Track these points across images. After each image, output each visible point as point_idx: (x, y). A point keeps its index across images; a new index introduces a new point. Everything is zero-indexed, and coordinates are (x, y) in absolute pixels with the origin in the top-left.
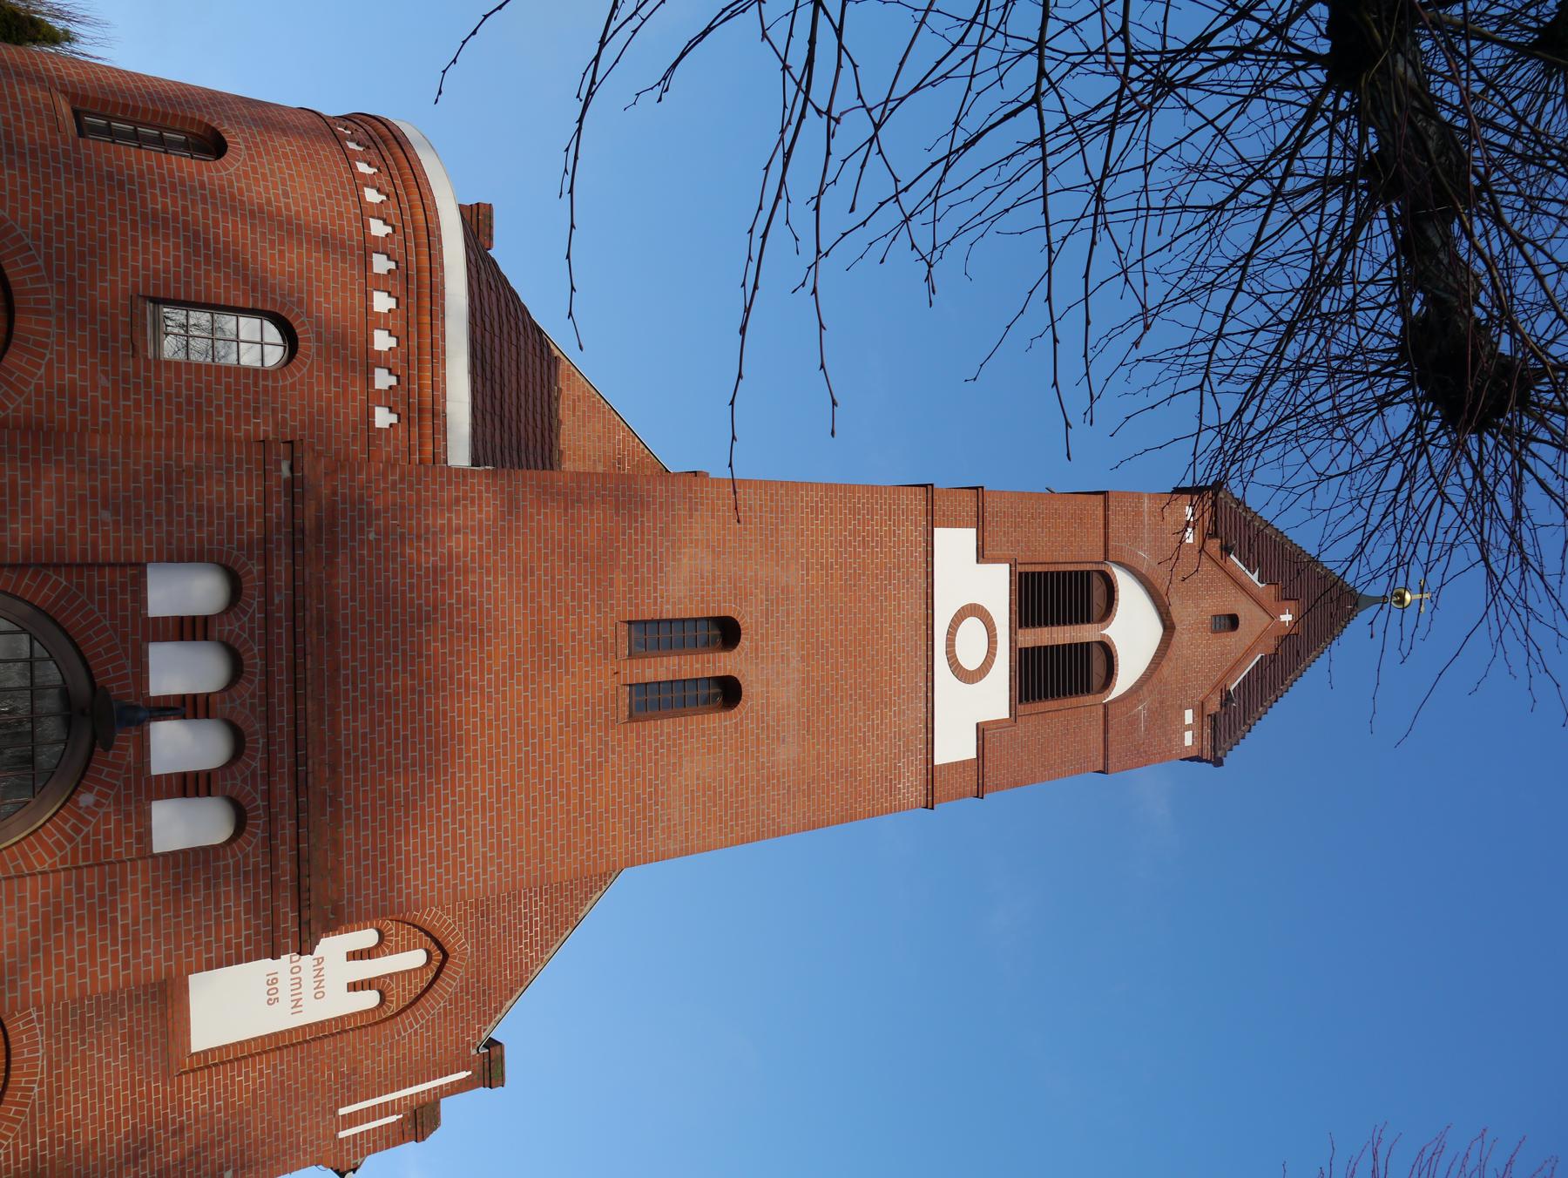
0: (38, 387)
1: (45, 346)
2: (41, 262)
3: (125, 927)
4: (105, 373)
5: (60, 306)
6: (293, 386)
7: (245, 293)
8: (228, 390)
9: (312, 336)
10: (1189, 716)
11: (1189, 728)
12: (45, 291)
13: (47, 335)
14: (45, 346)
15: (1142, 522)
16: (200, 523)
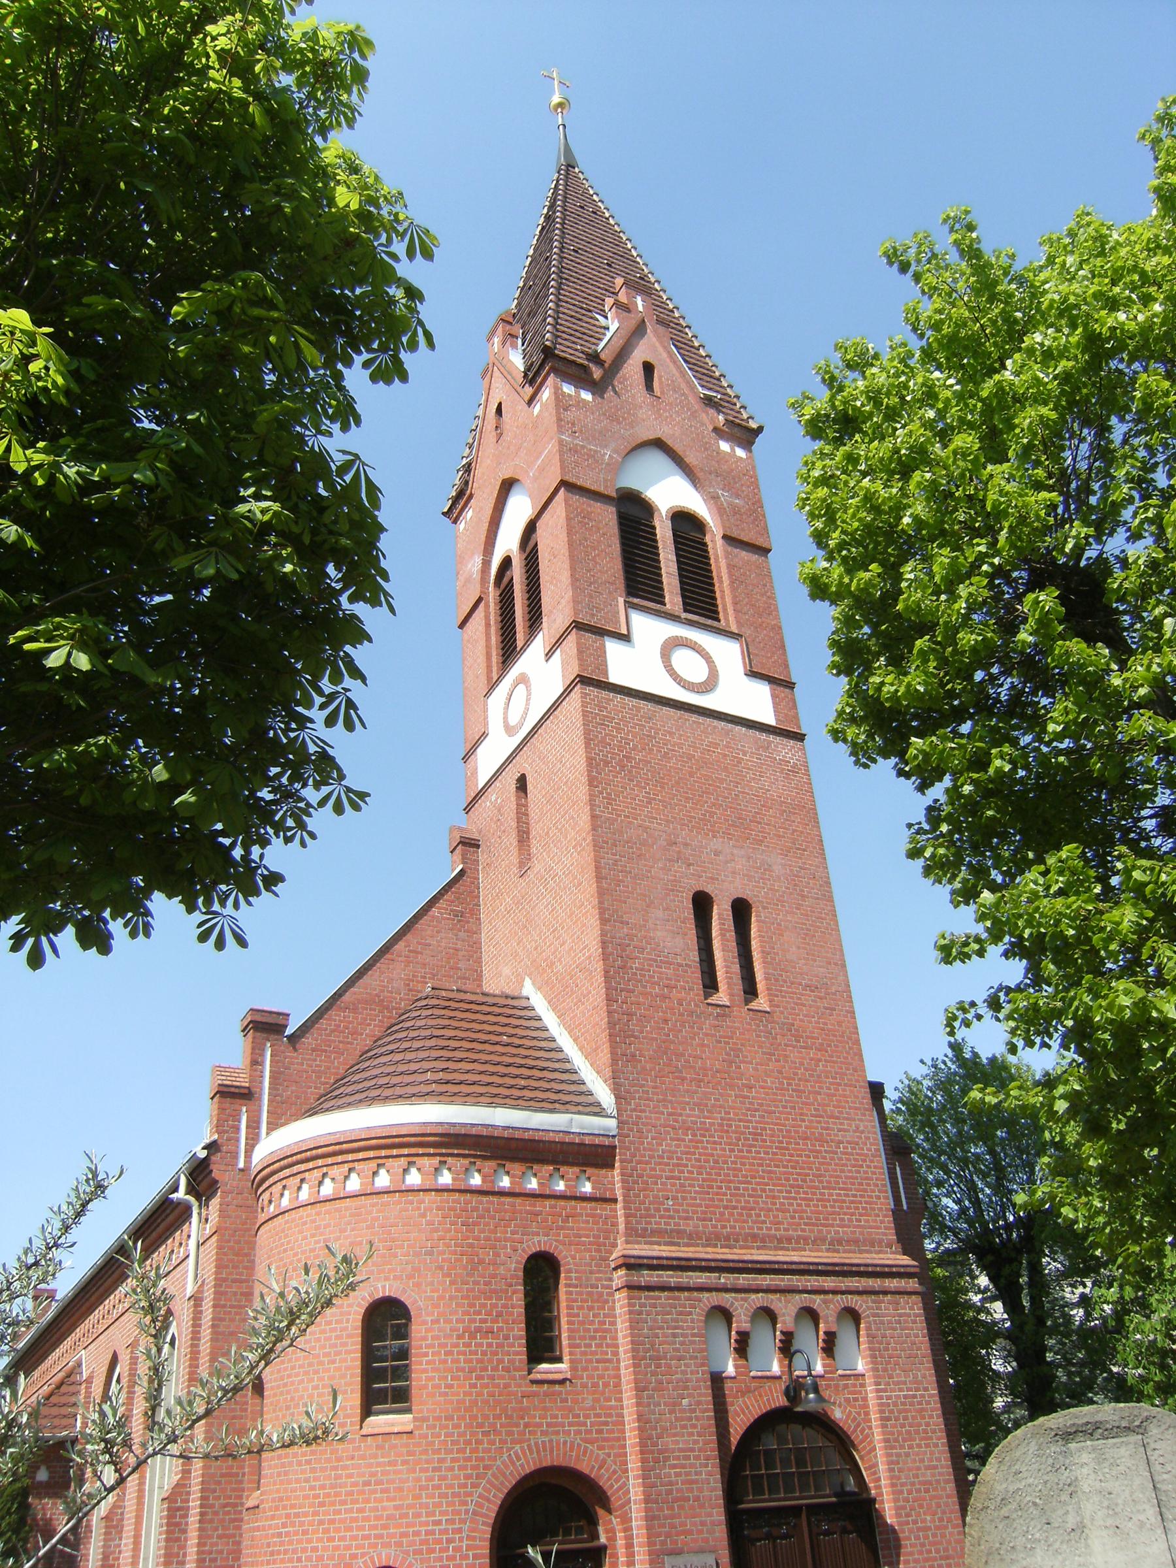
0: (601, 1448)
1: (572, 1444)
2: (517, 1447)
3: (909, 1390)
4: (583, 1400)
5: (544, 1433)
6: (574, 1258)
7: (514, 1292)
8: (581, 1308)
9: (536, 1239)
10: (725, 446)
11: (733, 450)
12: (536, 1444)
13: (565, 1443)
14: (572, 1444)
15: (583, 447)
16: (683, 1335)
